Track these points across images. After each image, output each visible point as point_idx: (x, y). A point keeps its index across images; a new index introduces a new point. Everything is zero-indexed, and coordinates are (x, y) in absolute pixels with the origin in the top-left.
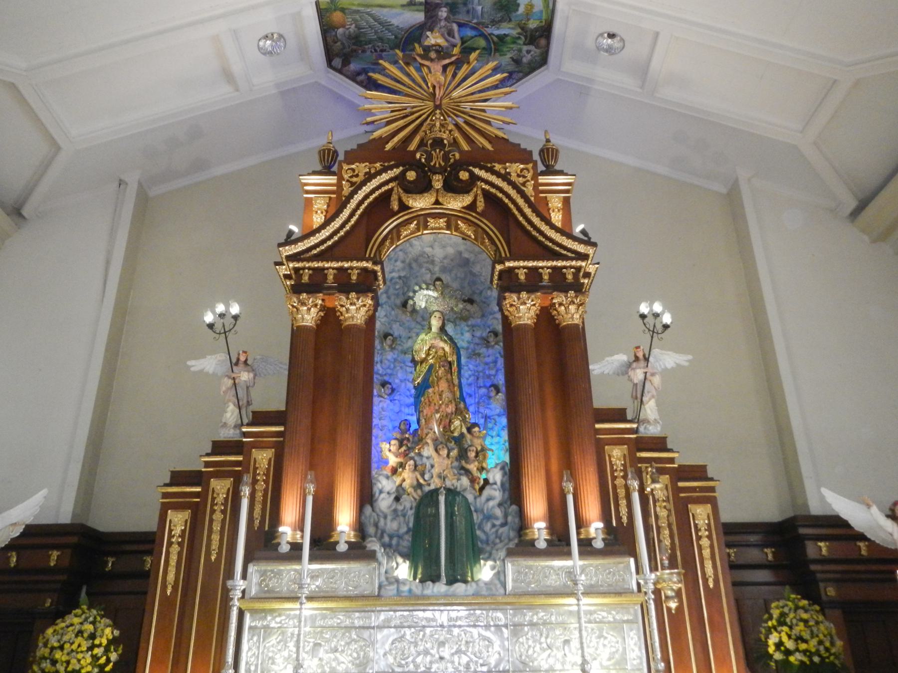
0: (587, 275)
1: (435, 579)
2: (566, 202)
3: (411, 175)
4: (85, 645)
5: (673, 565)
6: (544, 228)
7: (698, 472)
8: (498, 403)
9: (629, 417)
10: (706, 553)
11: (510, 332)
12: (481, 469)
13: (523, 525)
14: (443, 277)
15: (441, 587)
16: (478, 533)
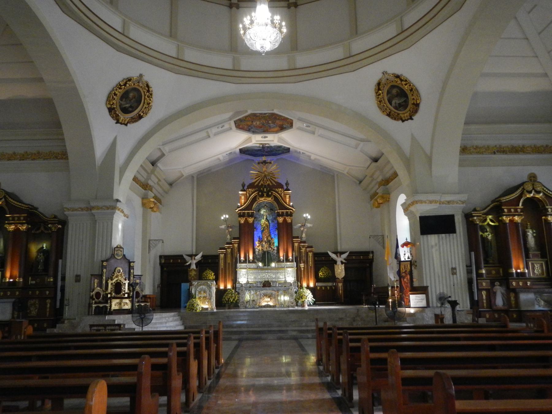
0: (293, 211)
1: (265, 266)
2: (290, 196)
3: (260, 193)
4: (211, 275)
5: (304, 262)
6: (285, 204)
7: (311, 247)
8: (277, 232)
9: (300, 237)
10: (311, 260)
11: (278, 223)
12: (273, 246)
13: (279, 257)
14: (267, 205)
15: (266, 267)
16: (272, 258)
